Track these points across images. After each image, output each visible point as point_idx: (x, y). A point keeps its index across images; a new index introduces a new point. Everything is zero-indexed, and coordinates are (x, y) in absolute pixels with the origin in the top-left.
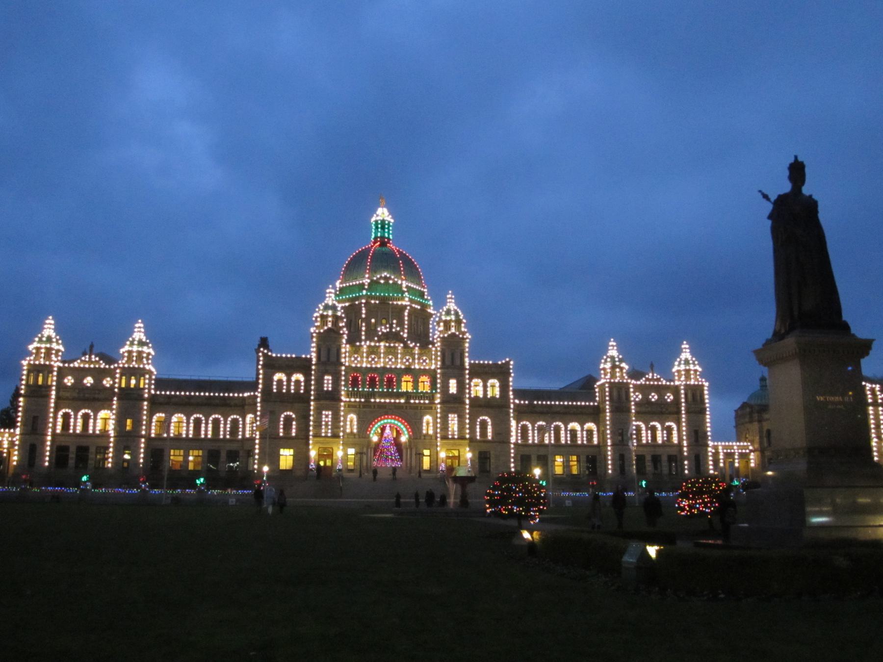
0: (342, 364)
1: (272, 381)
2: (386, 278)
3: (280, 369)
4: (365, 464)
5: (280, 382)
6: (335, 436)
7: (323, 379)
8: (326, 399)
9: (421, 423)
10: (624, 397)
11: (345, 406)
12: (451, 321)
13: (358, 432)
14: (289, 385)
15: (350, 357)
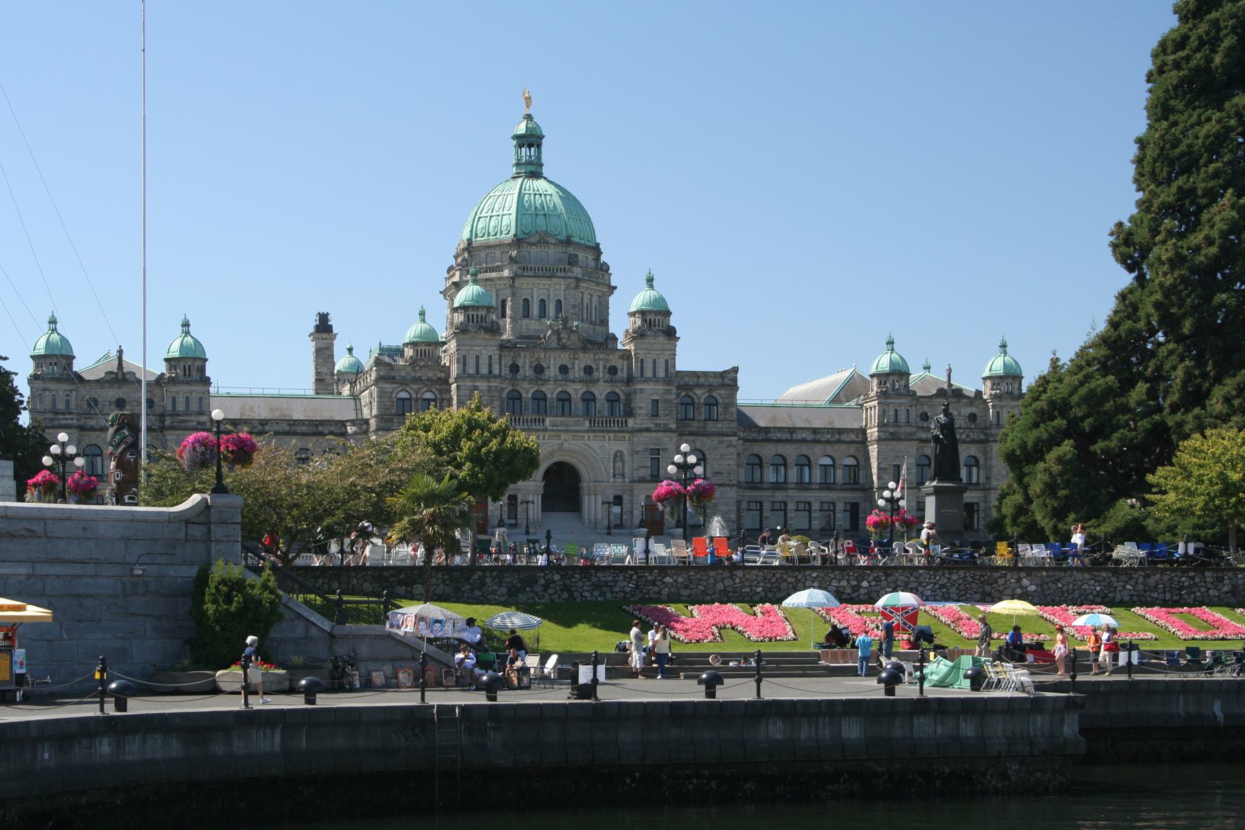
3: (404, 382)
10: (903, 418)
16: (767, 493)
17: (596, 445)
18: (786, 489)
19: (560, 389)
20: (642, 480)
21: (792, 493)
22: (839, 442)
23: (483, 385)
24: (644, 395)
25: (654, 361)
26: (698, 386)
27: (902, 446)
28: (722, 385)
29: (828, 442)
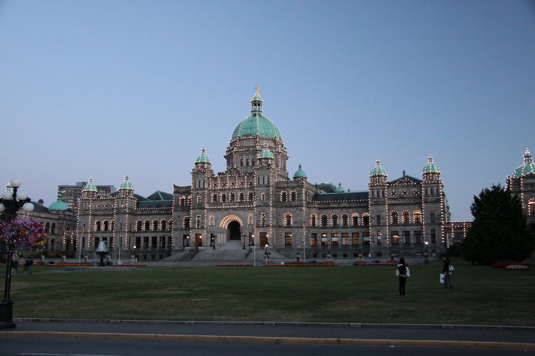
0: (205, 189)
1: (178, 200)
2: (248, 135)
3: (183, 193)
4: (219, 242)
5: (183, 200)
6: (203, 228)
7: (196, 198)
8: (198, 208)
9: (247, 218)
10: (381, 194)
11: (207, 212)
12: (262, 159)
13: (216, 225)
14: (186, 202)
15: (212, 184)
16: (329, 230)
17: (242, 213)
18: (337, 228)
19: (231, 192)
20: (258, 226)
21: (340, 230)
22: (360, 207)
23: (200, 192)
24: (259, 192)
25: (263, 178)
26: (288, 187)
27: (380, 207)
28: (298, 186)
29: (355, 207)
